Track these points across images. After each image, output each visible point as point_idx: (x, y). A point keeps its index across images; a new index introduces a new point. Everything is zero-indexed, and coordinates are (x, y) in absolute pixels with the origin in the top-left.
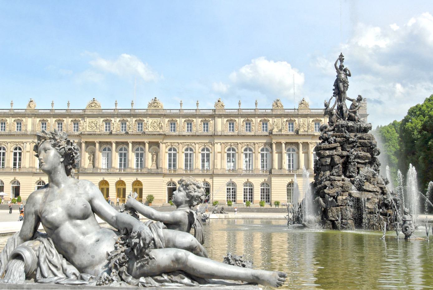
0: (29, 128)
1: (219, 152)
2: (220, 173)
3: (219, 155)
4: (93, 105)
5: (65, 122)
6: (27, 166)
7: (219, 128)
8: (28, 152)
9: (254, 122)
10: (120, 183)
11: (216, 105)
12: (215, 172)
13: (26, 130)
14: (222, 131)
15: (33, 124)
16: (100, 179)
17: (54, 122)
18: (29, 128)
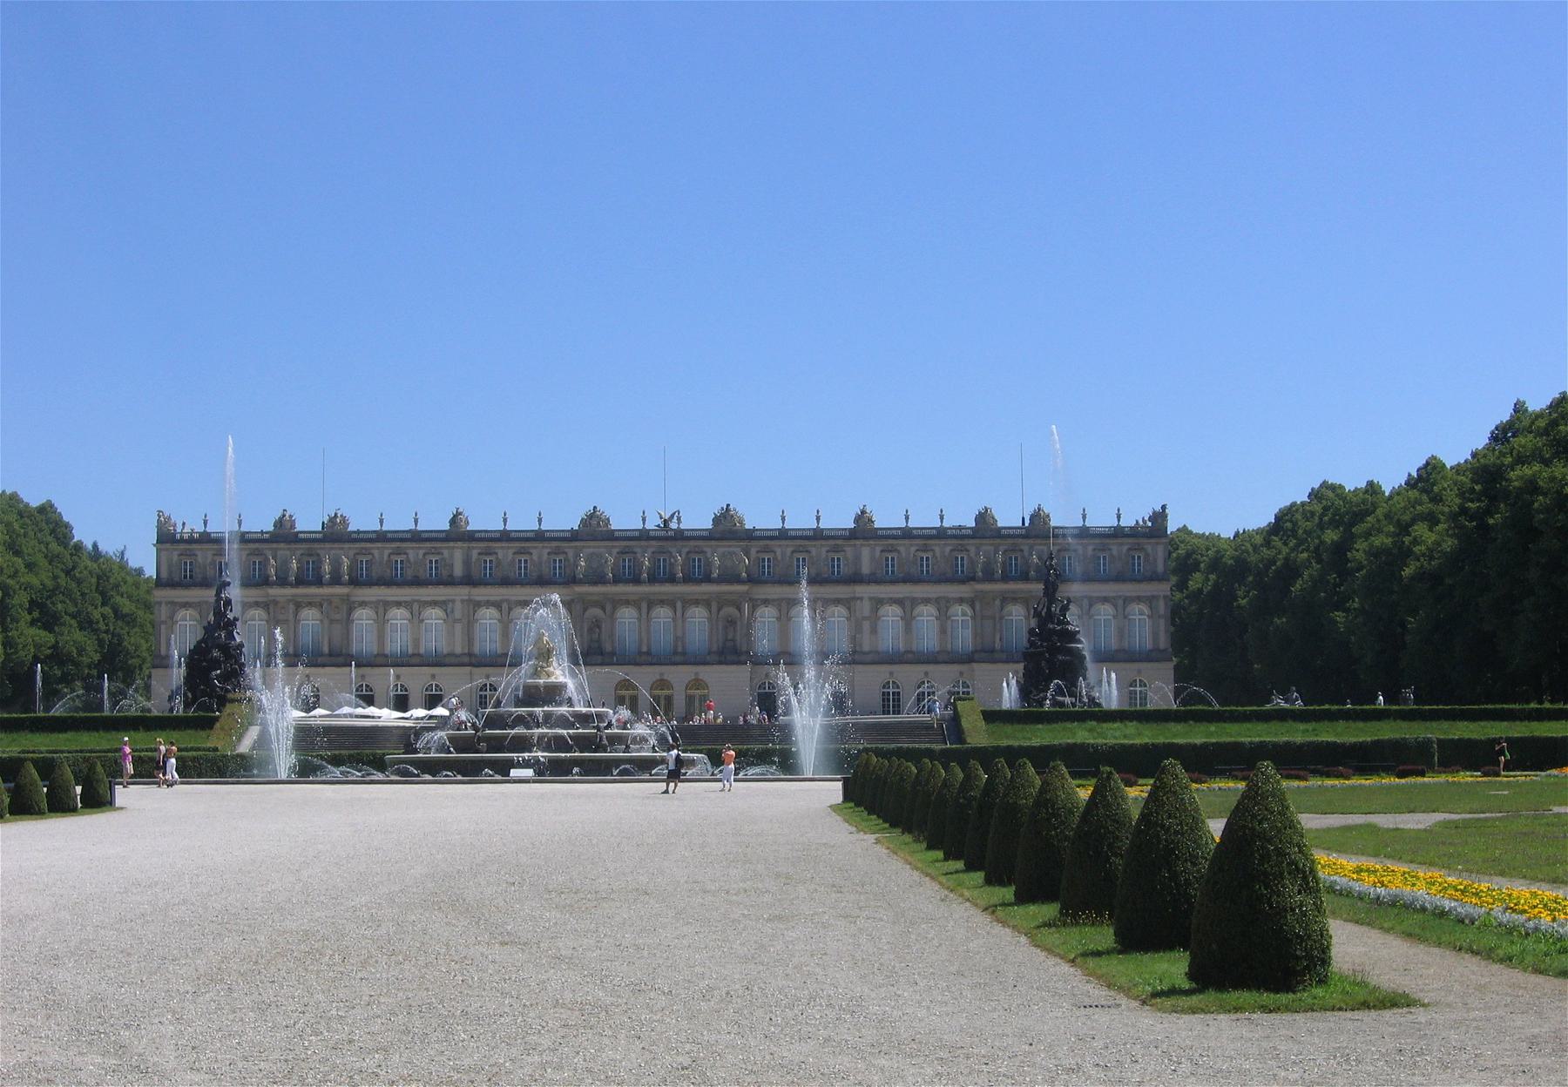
0: (458, 571)
1: (864, 618)
2: (869, 658)
3: (866, 625)
4: (594, 522)
5: (535, 557)
6: (458, 650)
7: (866, 569)
8: (455, 621)
10: (662, 683)
11: (858, 519)
12: (857, 657)
13: (451, 576)
14: (873, 574)
15: (467, 563)
16: (619, 673)
17: (510, 556)
18: (458, 571)
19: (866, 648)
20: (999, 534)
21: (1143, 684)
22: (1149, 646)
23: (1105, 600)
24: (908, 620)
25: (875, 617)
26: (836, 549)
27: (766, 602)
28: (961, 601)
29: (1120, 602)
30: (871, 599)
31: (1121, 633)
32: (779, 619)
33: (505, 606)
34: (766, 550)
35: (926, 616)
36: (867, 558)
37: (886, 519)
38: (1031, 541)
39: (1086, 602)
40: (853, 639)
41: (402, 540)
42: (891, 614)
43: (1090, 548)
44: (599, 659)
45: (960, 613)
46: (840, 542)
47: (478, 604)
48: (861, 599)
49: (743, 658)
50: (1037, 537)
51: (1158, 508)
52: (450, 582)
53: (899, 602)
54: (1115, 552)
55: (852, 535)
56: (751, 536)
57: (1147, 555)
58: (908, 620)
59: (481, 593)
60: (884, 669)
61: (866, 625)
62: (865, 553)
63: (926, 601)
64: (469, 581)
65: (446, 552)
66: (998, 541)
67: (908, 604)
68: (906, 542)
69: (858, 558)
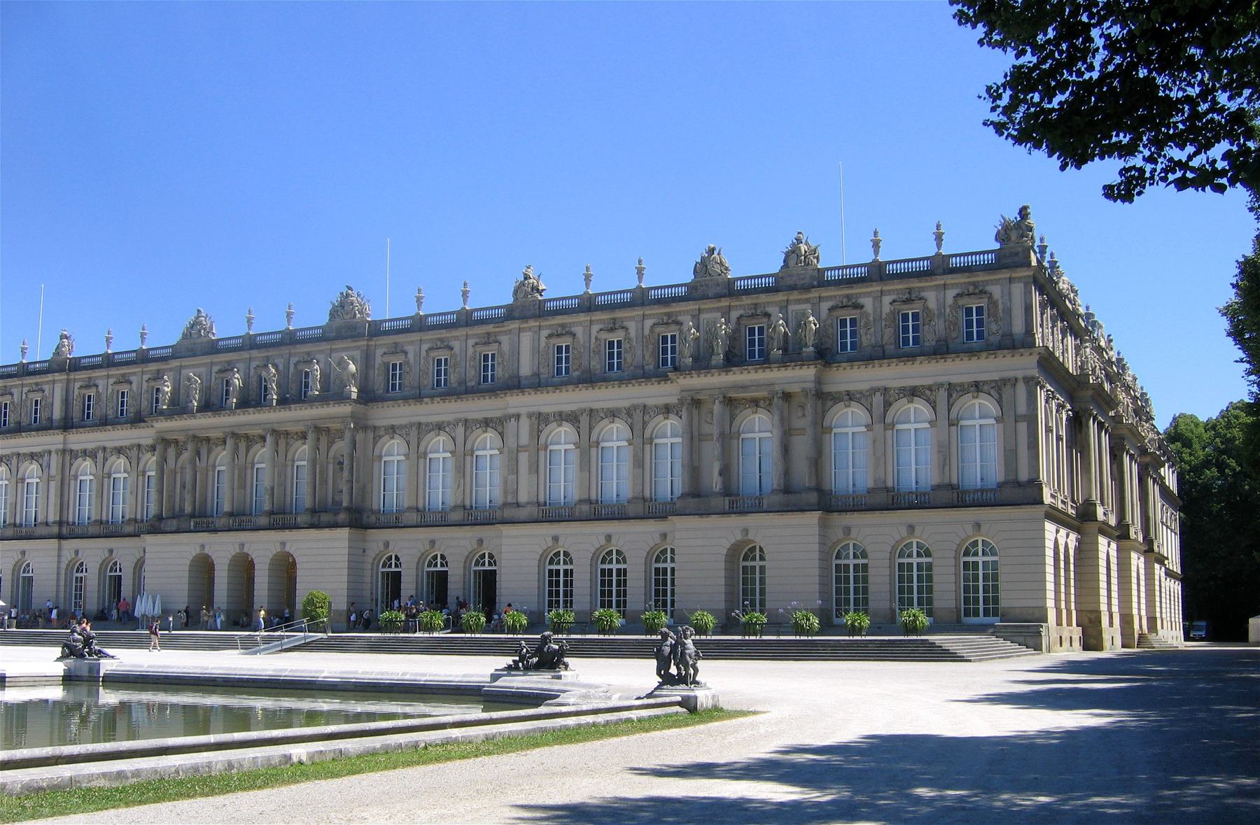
6: (51, 519)
7: (526, 370)
9: (633, 333)
13: (50, 419)
14: (537, 375)
18: (57, 414)
19: (523, 498)
20: (730, 290)
21: (989, 550)
22: (996, 473)
23: (913, 393)
24: (588, 448)
25: (538, 446)
26: (488, 340)
27: (393, 430)
28: (667, 410)
29: (942, 395)
30: (530, 416)
31: (945, 454)
32: (407, 456)
33: (100, 455)
34: (397, 349)
35: (615, 436)
36: (526, 349)
37: (558, 285)
38: (781, 297)
39: (878, 399)
40: (510, 487)
41: (10, 376)
42: (562, 438)
43: (887, 300)
44: (174, 524)
45: (669, 434)
46: (490, 328)
47: (74, 455)
48: (518, 416)
49: (342, 517)
50: (792, 288)
51: (1013, 215)
52: (47, 426)
53: (572, 418)
54: (932, 304)
55: (511, 313)
56: (376, 330)
57: (993, 303)
58: (588, 448)
59: (80, 440)
60: (599, 530)
61: (524, 458)
62: (526, 340)
63: (613, 414)
64: (67, 425)
65: (46, 388)
66: (724, 303)
67: (584, 420)
68: (583, 317)
69: (516, 352)
